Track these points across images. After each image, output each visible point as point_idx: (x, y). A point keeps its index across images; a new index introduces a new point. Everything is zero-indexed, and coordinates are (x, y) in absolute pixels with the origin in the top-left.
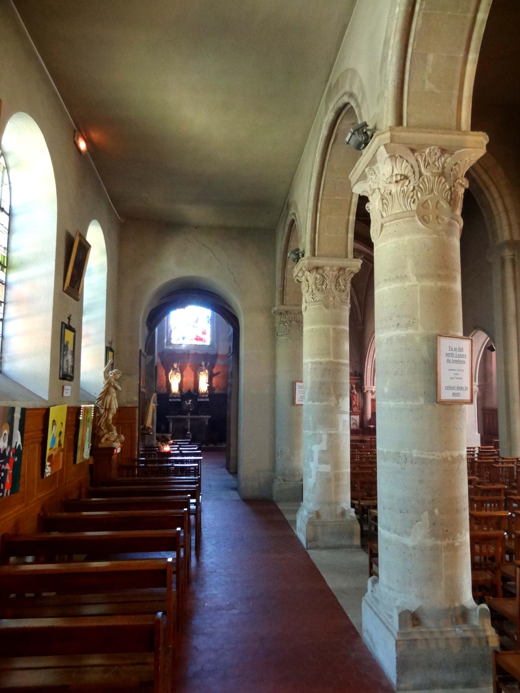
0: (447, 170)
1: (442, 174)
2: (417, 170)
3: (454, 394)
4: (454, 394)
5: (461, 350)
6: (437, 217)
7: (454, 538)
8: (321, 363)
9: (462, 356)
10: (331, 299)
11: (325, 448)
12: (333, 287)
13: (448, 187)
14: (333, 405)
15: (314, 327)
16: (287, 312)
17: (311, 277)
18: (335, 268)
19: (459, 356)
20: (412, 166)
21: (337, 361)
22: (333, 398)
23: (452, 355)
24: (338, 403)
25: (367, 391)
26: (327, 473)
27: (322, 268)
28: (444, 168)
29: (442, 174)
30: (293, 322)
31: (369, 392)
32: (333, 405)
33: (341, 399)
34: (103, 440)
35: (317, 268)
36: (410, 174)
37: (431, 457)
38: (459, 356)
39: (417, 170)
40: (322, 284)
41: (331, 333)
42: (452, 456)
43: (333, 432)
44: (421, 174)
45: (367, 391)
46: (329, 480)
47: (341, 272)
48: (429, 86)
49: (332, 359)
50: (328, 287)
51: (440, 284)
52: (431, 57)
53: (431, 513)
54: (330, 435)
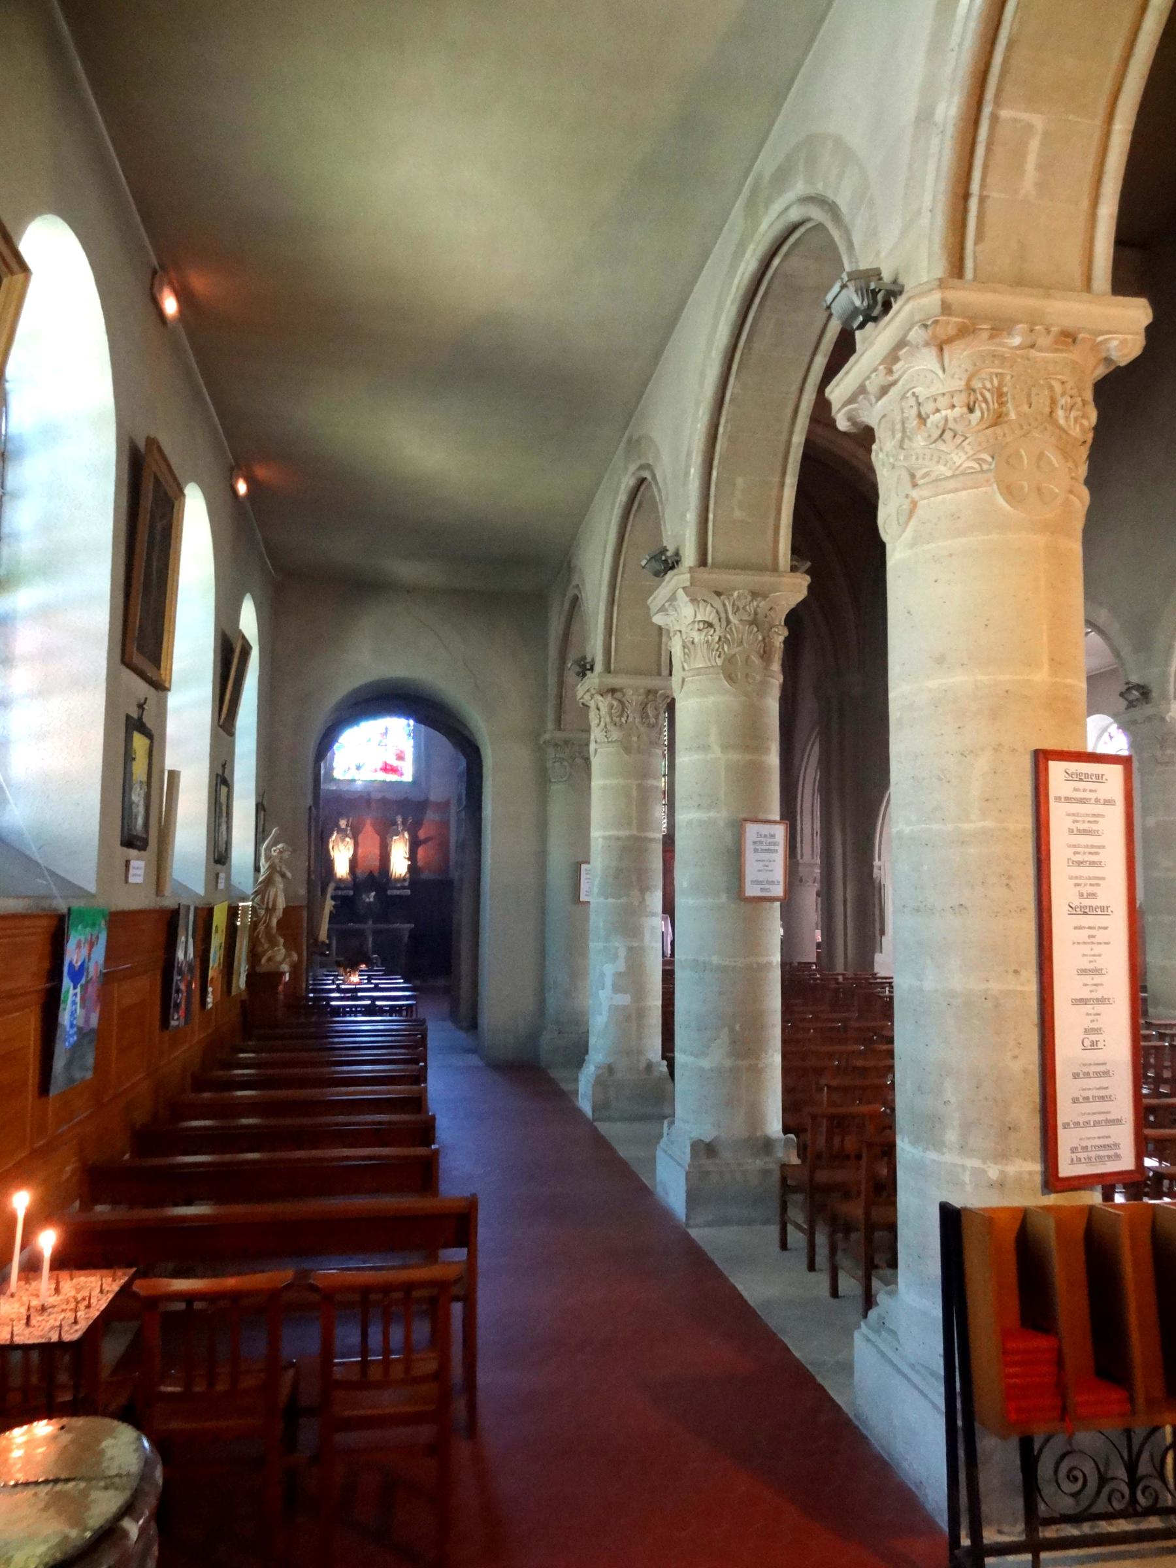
0: (760, 617)
1: (754, 622)
2: (723, 615)
5: (773, 836)
6: (747, 675)
7: (758, 1058)
8: (618, 838)
9: (775, 844)
10: (635, 739)
11: (622, 969)
12: (637, 720)
13: (760, 638)
14: (636, 903)
15: (608, 782)
16: (566, 742)
17: (604, 703)
18: (642, 691)
19: (770, 844)
20: (717, 612)
21: (643, 835)
22: (635, 893)
23: (761, 843)
24: (644, 900)
26: (624, 1008)
27: (621, 690)
28: (756, 614)
29: (754, 622)
32: (636, 903)
33: (647, 895)
34: (264, 960)
35: (613, 691)
36: (715, 622)
37: (733, 964)
38: (770, 844)
39: (723, 615)
40: (621, 716)
41: (634, 793)
42: (758, 964)
43: (636, 945)
44: (728, 622)
46: (628, 1018)
47: (651, 697)
48: (738, 514)
49: (635, 832)
50: (630, 719)
51: (748, 757)
52: (740, 481)
53: (732, 1030)
54: (630, 949)
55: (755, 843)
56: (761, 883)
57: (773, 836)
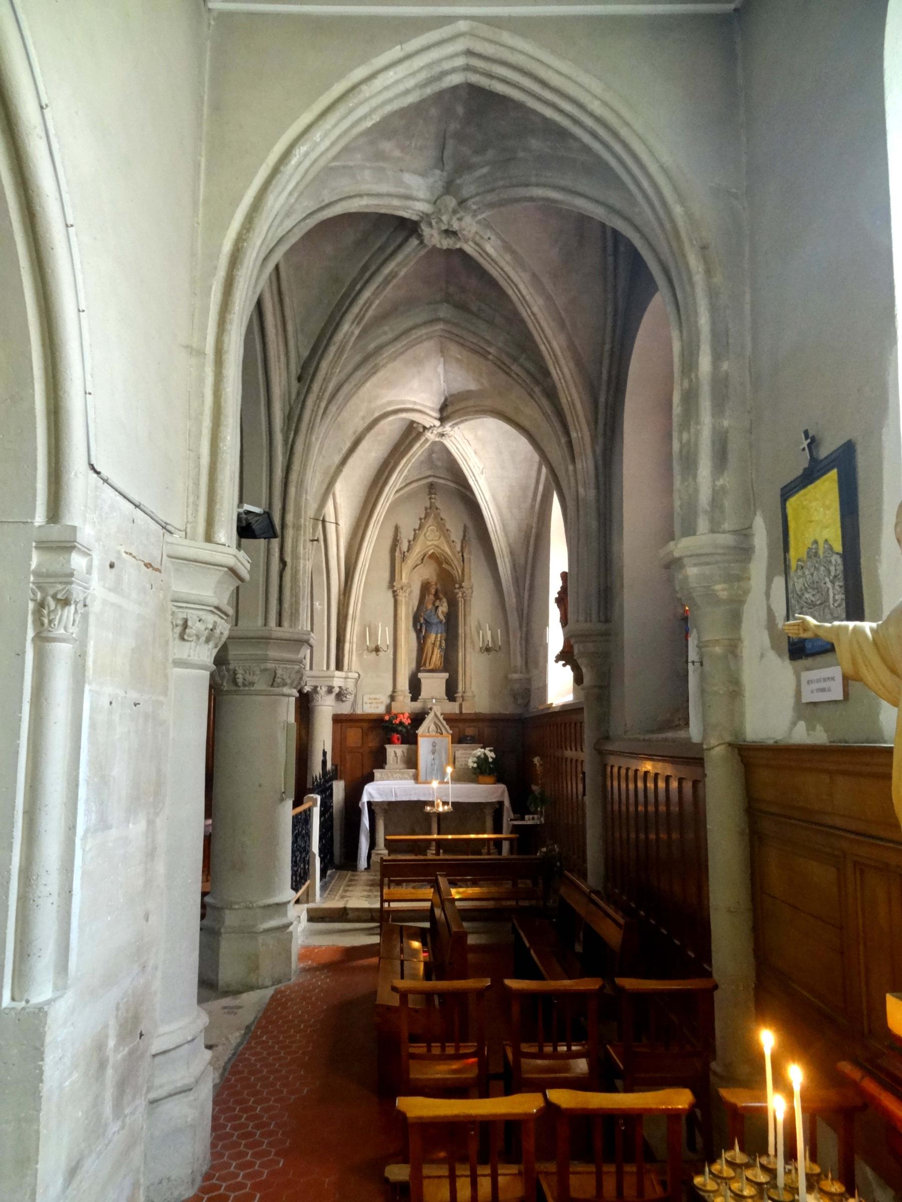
25: (315, 688)
31: (323, 691)
45: (315, 688)
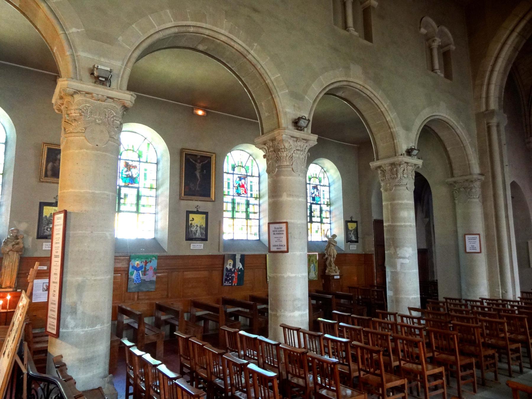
3: (277, 248)
4: (277, 248)
5: (281, 228)
7: (277, 311)
9: (282, 231)
16: (455, 182)
19: (280, 231)
24: (396, 252)
30: (461, 189)
38: (280, 231)
41: (389, 207)
49: (390, 224)
55: (274, 231)
56: (277, 246)
57: (281, 228)
